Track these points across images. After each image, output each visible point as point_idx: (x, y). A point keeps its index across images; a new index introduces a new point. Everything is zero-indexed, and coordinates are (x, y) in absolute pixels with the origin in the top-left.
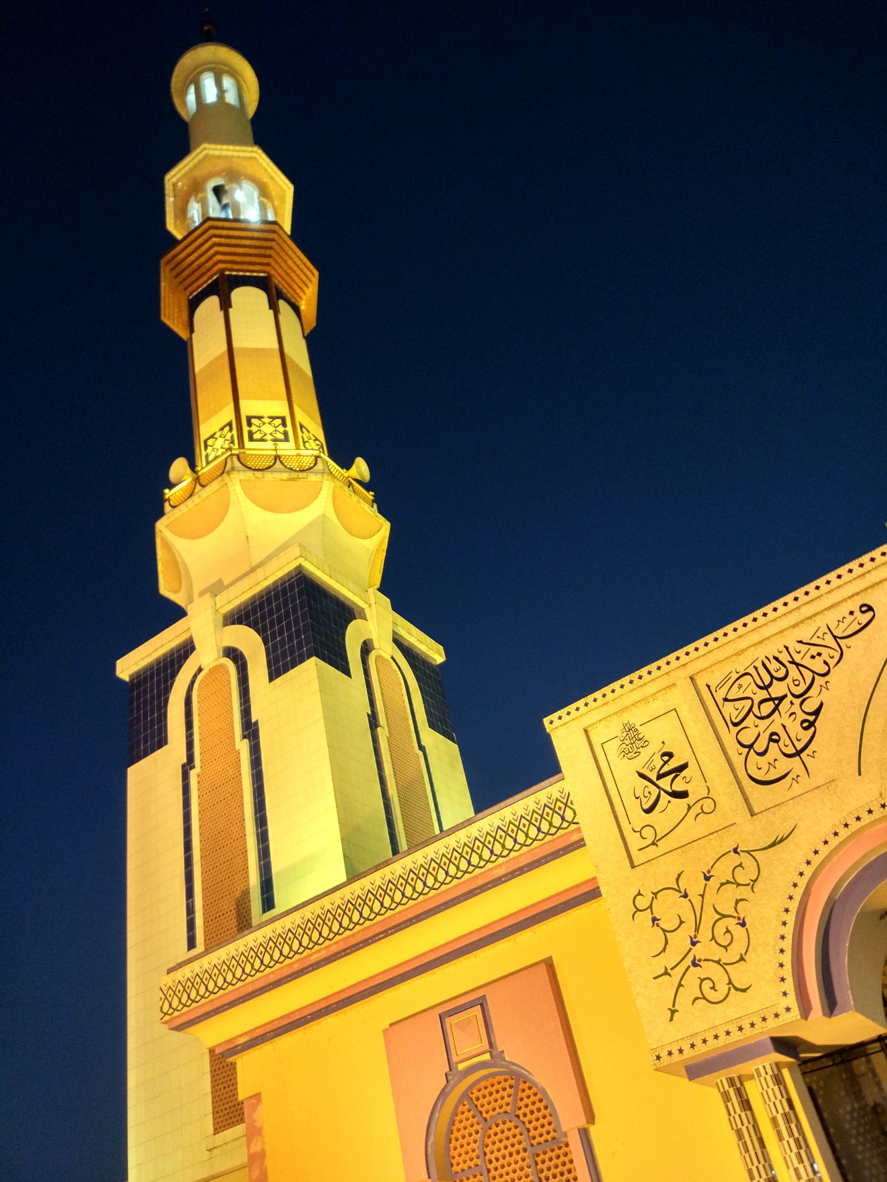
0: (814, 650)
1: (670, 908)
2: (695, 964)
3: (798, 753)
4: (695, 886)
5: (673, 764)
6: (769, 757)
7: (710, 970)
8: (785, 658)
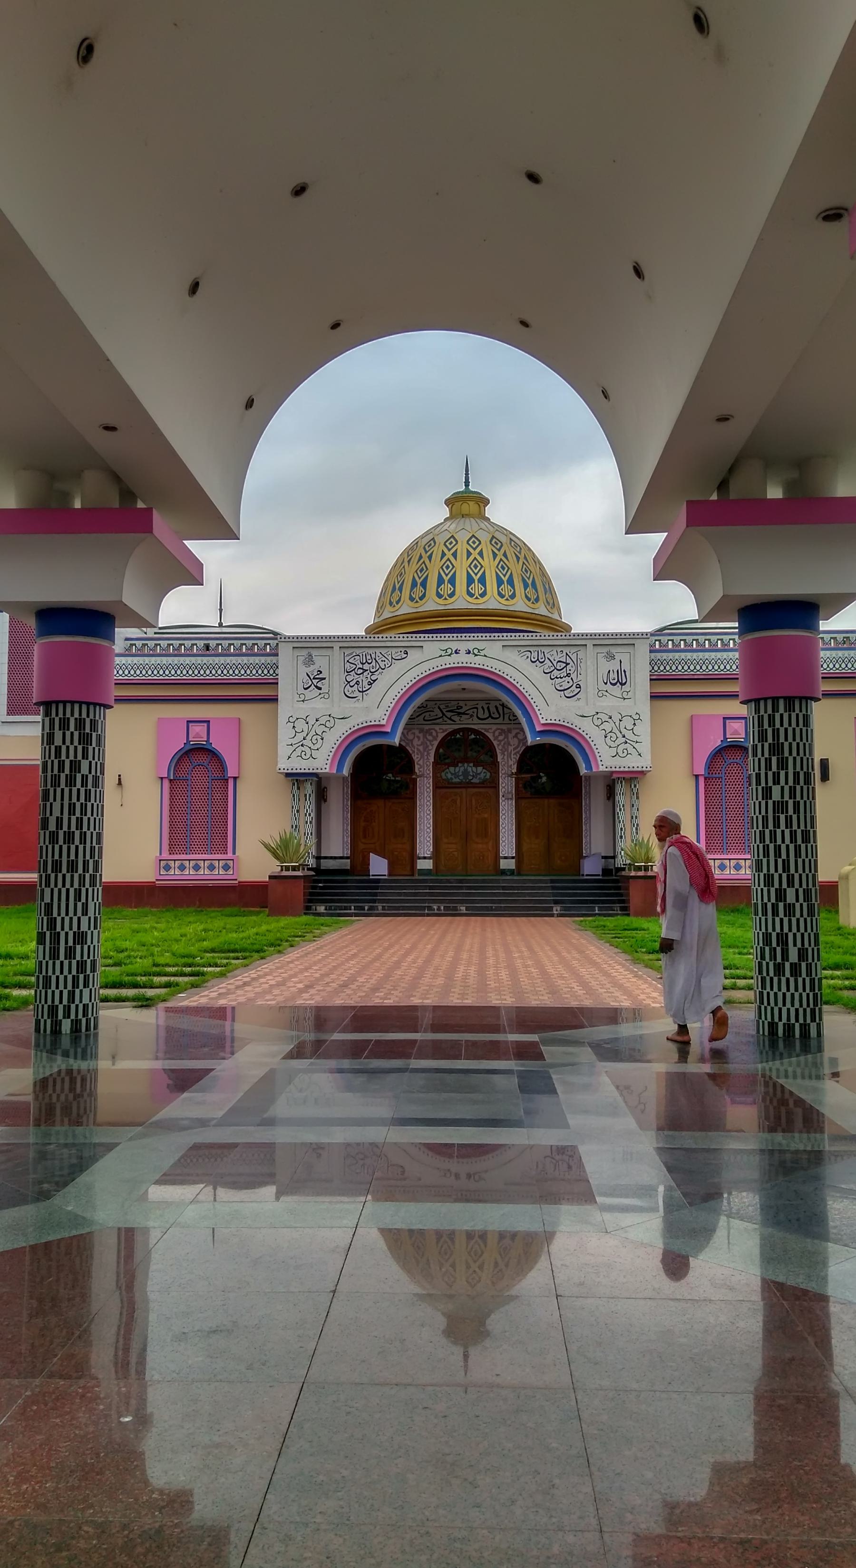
0: (384, 659)
1: (300, 725)
2: (302, 745)
3: (363, 692)
4: (311, 722)
5: (320, 676)
6: (353, 689)
7: (305, 749)
8: (373, 656)
